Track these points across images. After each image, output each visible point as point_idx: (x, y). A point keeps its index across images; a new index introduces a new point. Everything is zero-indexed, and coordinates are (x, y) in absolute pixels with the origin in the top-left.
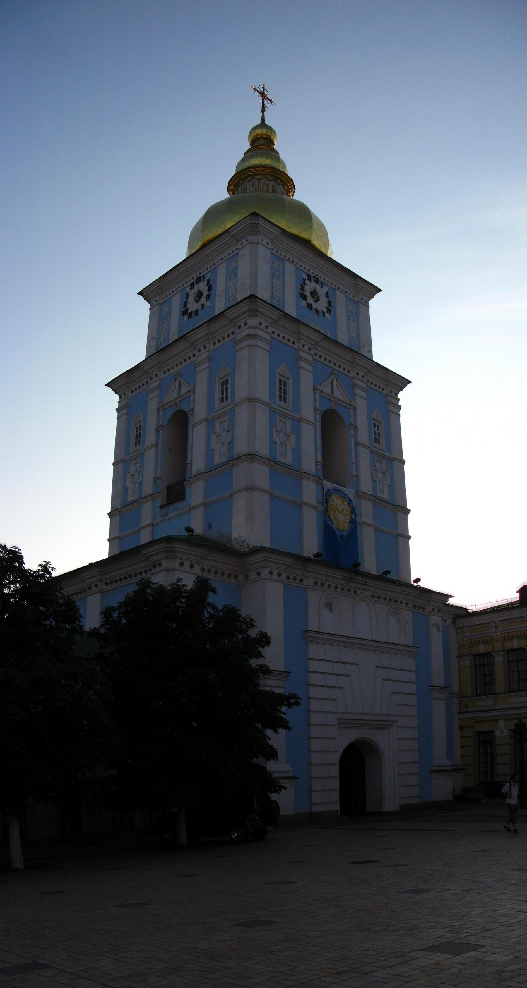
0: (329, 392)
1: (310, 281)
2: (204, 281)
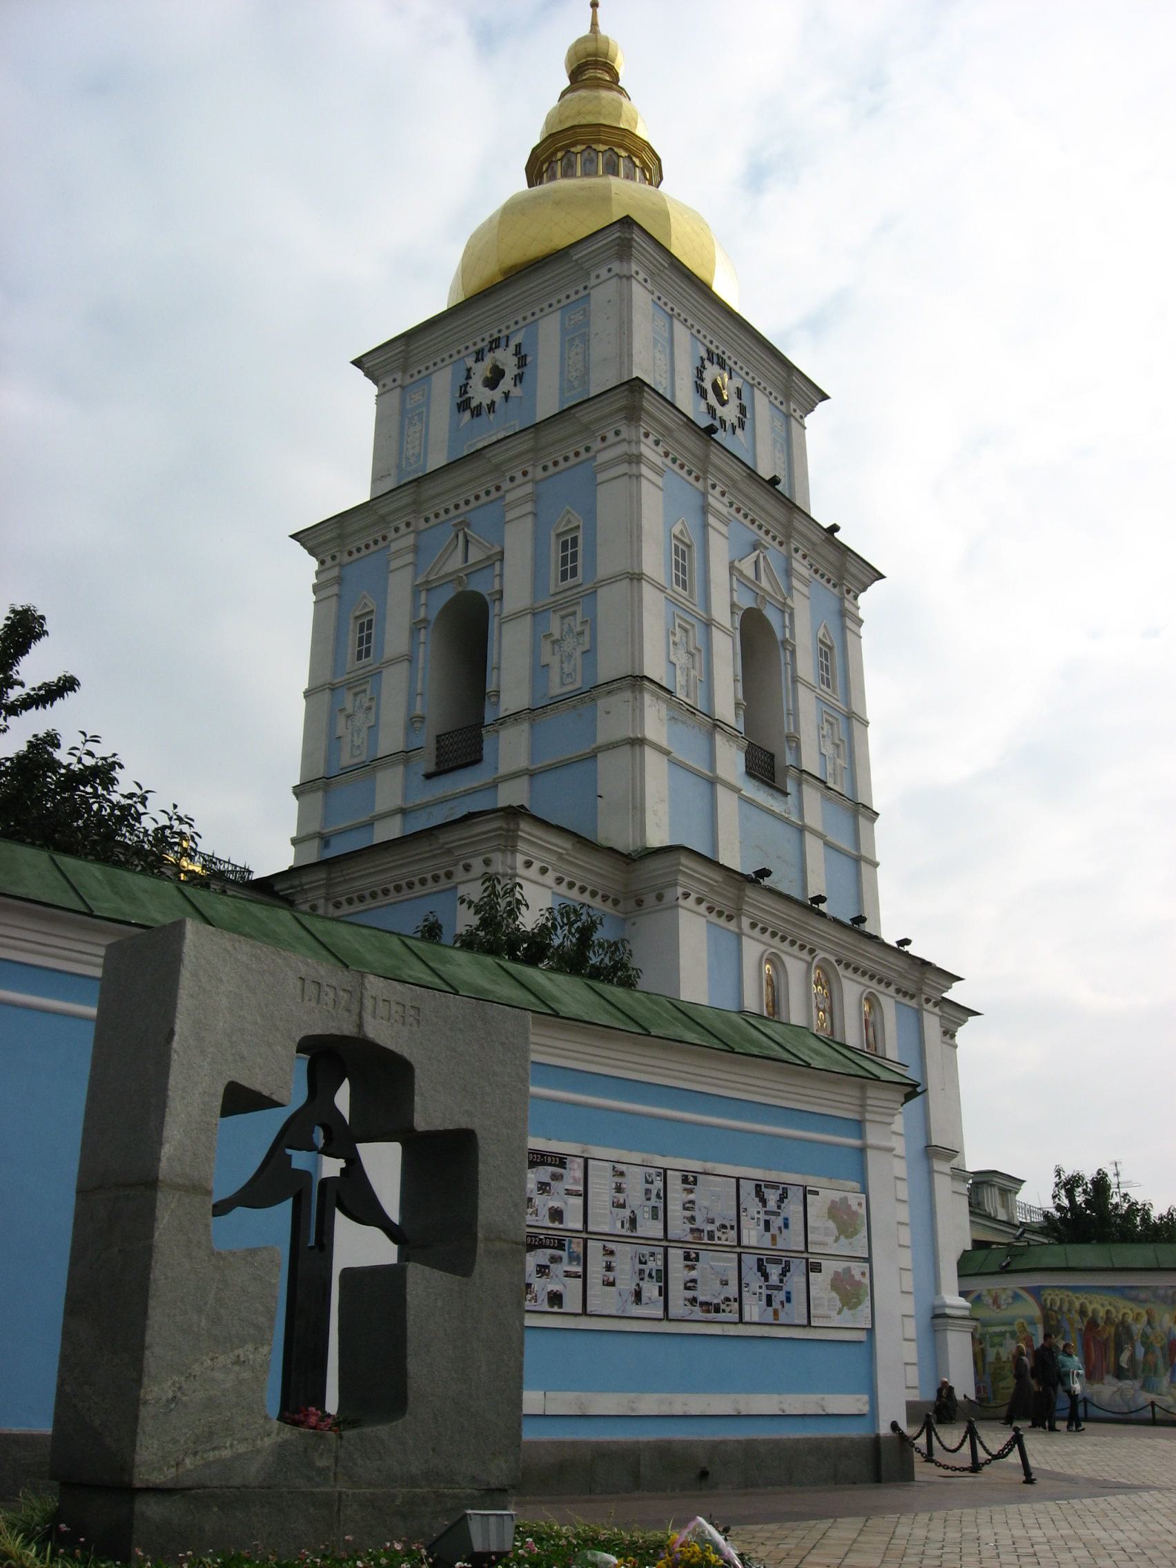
0: (752, 577)
1: (713, 363)
2: (507, 346)
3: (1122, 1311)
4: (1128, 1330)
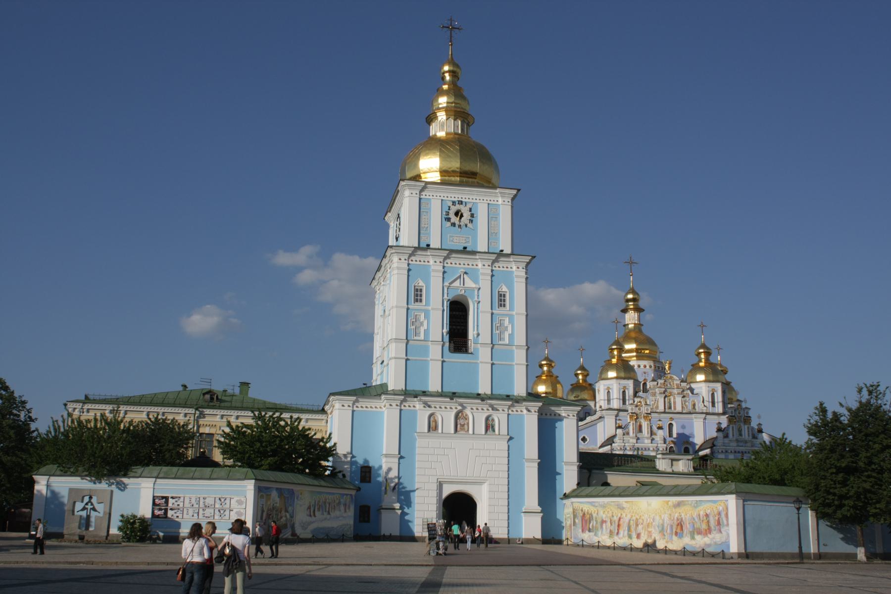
4: (592, 516)
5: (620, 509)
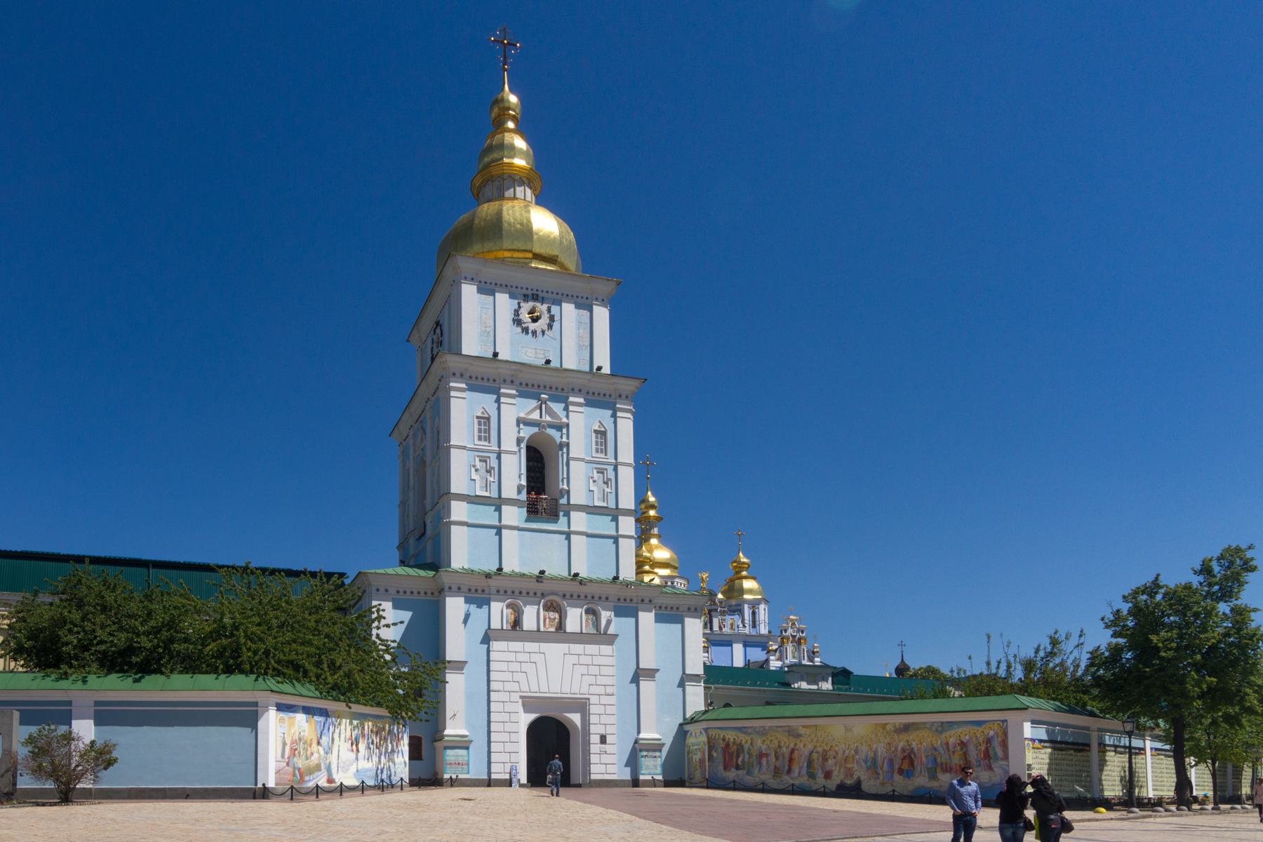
3: (740, 738)
5: (794, 736)
